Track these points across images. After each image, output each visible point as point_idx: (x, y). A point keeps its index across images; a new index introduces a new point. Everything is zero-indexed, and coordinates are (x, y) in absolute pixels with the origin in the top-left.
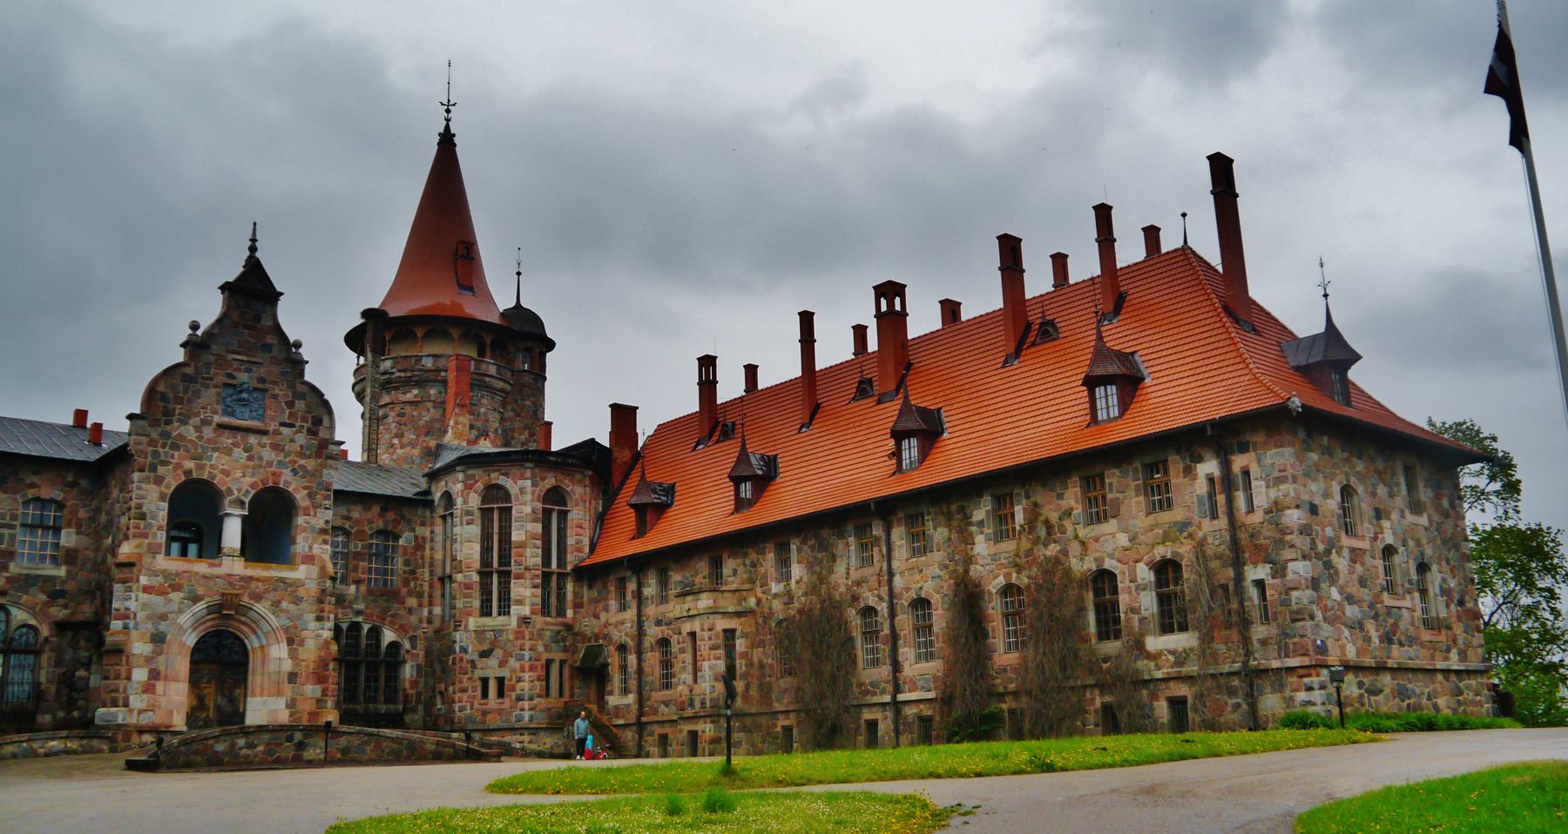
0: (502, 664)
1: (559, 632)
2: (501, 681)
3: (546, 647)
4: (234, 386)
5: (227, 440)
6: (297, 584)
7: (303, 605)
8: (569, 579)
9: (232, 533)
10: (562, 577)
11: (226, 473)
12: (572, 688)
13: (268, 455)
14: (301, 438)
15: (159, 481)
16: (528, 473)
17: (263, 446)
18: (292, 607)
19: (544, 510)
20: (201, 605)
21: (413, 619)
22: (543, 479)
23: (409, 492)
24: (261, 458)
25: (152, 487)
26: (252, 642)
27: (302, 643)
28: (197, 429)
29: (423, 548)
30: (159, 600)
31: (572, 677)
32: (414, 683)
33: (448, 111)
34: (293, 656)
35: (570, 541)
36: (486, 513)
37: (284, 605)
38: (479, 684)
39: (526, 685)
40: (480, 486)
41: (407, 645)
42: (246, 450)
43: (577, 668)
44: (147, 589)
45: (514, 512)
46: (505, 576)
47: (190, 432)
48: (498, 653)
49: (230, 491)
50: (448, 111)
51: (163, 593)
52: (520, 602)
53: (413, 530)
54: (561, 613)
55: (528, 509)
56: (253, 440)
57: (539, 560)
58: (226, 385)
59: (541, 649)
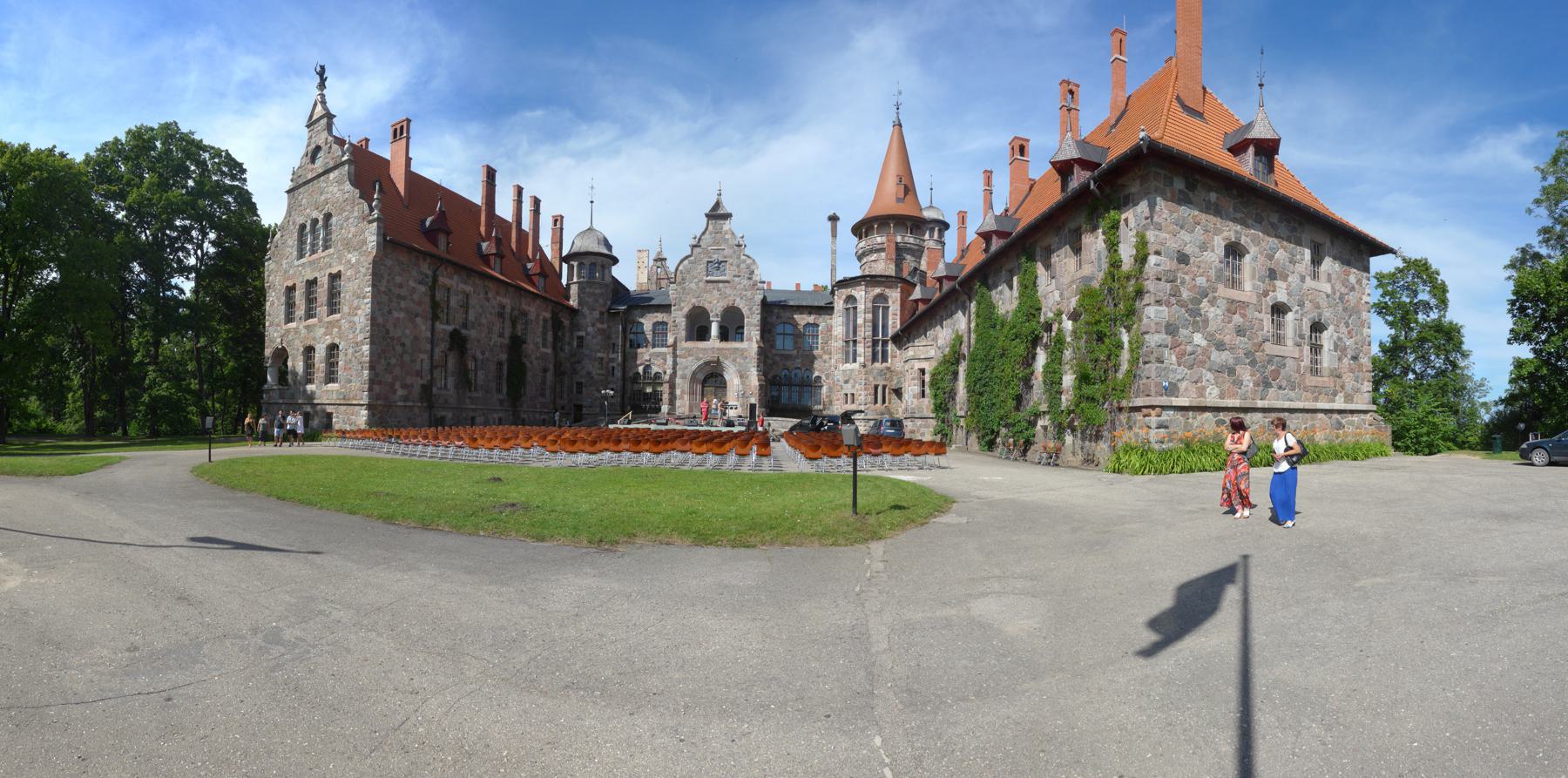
0: (853, 387)
1: (882, 371)
2: (853, 395)
3: (874, 378)
4: (711, 262)
5: (710, 286)
6: (743, 350)
7: (747, 360)
8: (890, 342)
9: (714, 330)
10: (885, 343)
11: (710, 303)
12: (890, 400)
13: (728, 291)
14: (745, 282)
15: (681, 309)
16: (863, 287)
17: (726, 287)
18: (742, 361)
19: (874, 307)
20: (702, 362)
21: (826, 365)
22: (873, 290)
23: (822, 304)
24: (725, 293)
25: (679, 312)
26: (727, 377)
27: (747, 378)
28: (697, 284)
29: (831, 331)
30: (684, 360)
31: (890, 393)
32: (827, 397)
33: (898, 109)
34: (743, 383)
35: (890, 323)
36: (847, 309)
37: (738, 360)
38: (843, 396)
39: (862, 397)
40: (844, 297)
41: (824, 378)
42: (718, 291)
43: (893, 390)
44: (681, 357)
45: (858, 310)
46: (855, 342)
47: (693, 286)
48: (851, 381)
49: (712, 311)
50: (898, 109)
51: (685, 358)
52: (860, 356)
53: (826, 322)
54: (885, 359)
55: (863, 307)
56: (721, 285)
57: (870, 333)
58: (708, 262)
59: (871, 379)
